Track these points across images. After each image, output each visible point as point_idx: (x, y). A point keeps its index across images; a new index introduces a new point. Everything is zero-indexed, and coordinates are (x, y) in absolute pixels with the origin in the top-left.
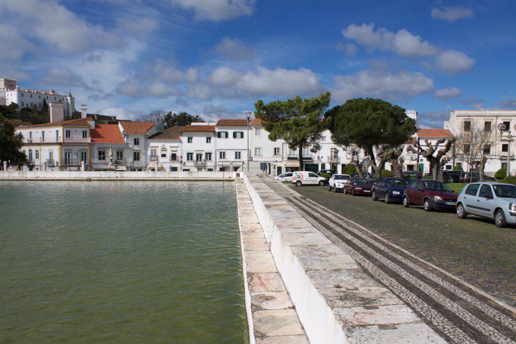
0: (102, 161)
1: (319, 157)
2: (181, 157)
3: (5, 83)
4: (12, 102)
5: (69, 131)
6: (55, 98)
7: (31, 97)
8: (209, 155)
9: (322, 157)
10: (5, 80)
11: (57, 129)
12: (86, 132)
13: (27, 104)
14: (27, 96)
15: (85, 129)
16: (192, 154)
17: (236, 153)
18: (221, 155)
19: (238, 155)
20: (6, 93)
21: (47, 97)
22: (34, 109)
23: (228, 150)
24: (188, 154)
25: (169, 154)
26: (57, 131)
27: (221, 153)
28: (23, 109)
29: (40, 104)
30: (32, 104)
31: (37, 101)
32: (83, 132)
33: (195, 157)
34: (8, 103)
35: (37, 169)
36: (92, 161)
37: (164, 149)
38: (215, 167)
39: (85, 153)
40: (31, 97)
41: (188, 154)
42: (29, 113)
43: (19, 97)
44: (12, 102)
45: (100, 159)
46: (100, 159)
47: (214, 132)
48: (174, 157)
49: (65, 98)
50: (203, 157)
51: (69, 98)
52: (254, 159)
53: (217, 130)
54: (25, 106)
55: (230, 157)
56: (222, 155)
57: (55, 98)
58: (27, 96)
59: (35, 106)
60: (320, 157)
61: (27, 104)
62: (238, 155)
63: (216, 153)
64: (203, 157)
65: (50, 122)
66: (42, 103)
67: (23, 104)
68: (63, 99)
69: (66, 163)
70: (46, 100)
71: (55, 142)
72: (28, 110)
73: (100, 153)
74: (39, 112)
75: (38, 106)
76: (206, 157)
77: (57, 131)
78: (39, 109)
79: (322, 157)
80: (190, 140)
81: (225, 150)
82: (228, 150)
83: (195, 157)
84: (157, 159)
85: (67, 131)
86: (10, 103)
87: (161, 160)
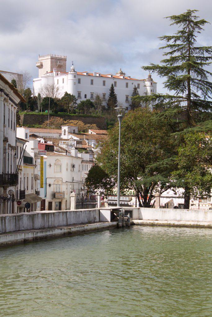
3: (52, 62)
4: (66, 94)
6: (127, 84)
7: (92, 83)
10: (52, 58)
13: (86, 96)
14: (86, 81)
20: (56, 79)
21: (115, 83)
22: (96, 103)
28: (83, 103)
29: (104, 95)
30: (92, 95)
31: (100, 90)
34: (60, 95)
40: (92, 83)
42: (92, 110)
43: (75, 84)
44: (66, 94)
49: (142, 84)
51: (148, 83)
54: (83, 99)
57: (127, 84)
58: (86, 81)
59: (98, 97)
61: (86, 96)
66: (108, 93)
67: (79, 96)
68: (139, 85)
70: (115, 88)
72: (88, 105)
74: (104, 108)
75: (101, 96)
78: (104, 104)
86: (63, 95)
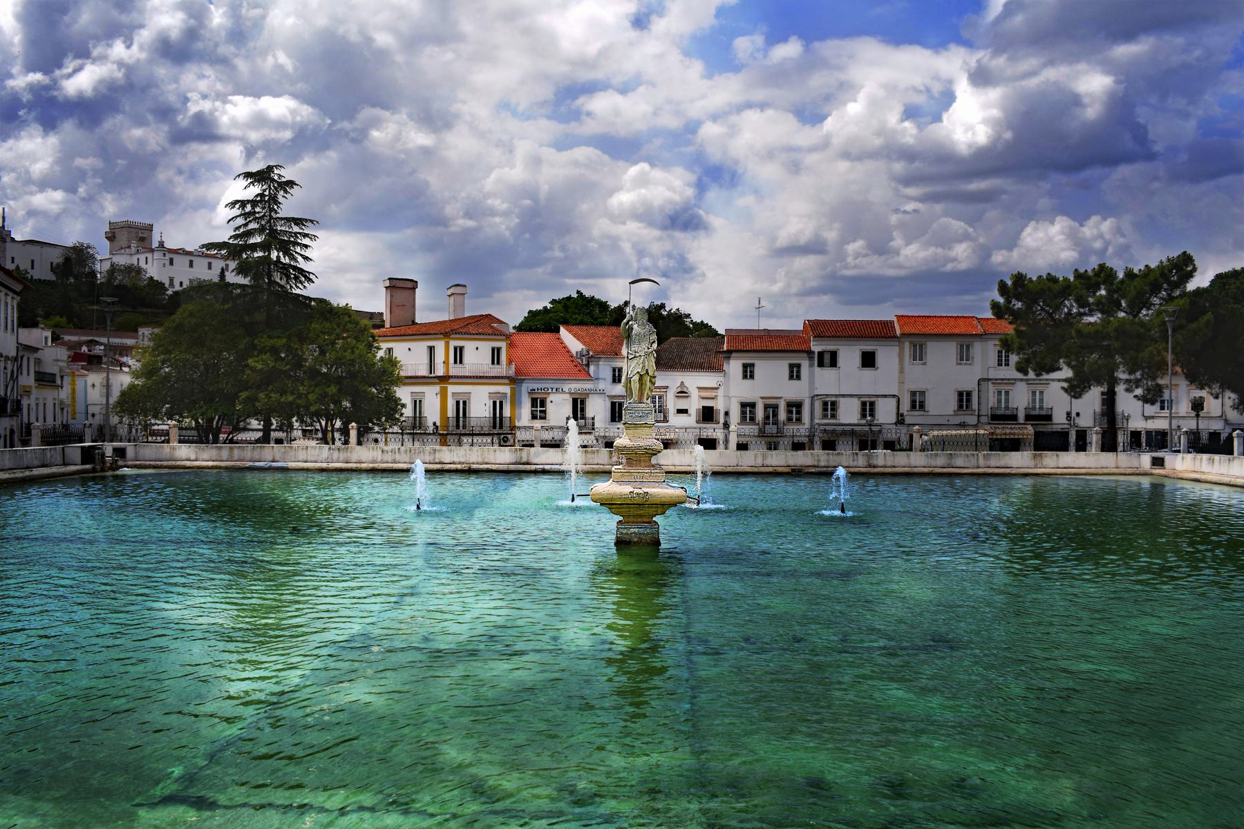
0: (538, 424)
1: (1069, 414)
2: (727, 414)
5: (461, 349)
8: (795, 407)
9: (1078, 414)
11: (431, 343)
12: (499, 349)
15: (497, 344)
16: (753, 405)
17: (864, 404)
18: (825, 410)
19: (868, 408)
23: (844, 396)
24: (743, 405)
25: (695, 404)
26: (431, 349)
27: (825, 404)
32: (493, 349)
33: (760, 414)
35: (376, 441)
36: (517, 424)
37: (683, 393)
38: (811, 438)
39: (465, 403)
41: (743, 405)
45: (534, 417)
46: (534, 417)
47: (810, 353)
48: (708, 415)
50: (782, 416)
52: (908, 420)
53: (816, 347)
55: (849, 414)
56: (830, 407)
60: (1074, 415)
62: (868, 408)
63: (812, 404)
64: (782, 416)
65: (383, 326)
69: (458, 427)
71: (423, 371)
73: (534, 402)
76: (790, 412)
77: (431, 349)
79: (1078, 414)
80: (748, 372)
81: (836, 396)
82: (844, 396)
83: (760, 414)
84: (665, 420)
85: (455, 349)
87: (675, 420)
